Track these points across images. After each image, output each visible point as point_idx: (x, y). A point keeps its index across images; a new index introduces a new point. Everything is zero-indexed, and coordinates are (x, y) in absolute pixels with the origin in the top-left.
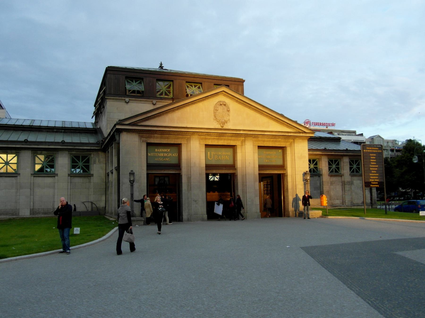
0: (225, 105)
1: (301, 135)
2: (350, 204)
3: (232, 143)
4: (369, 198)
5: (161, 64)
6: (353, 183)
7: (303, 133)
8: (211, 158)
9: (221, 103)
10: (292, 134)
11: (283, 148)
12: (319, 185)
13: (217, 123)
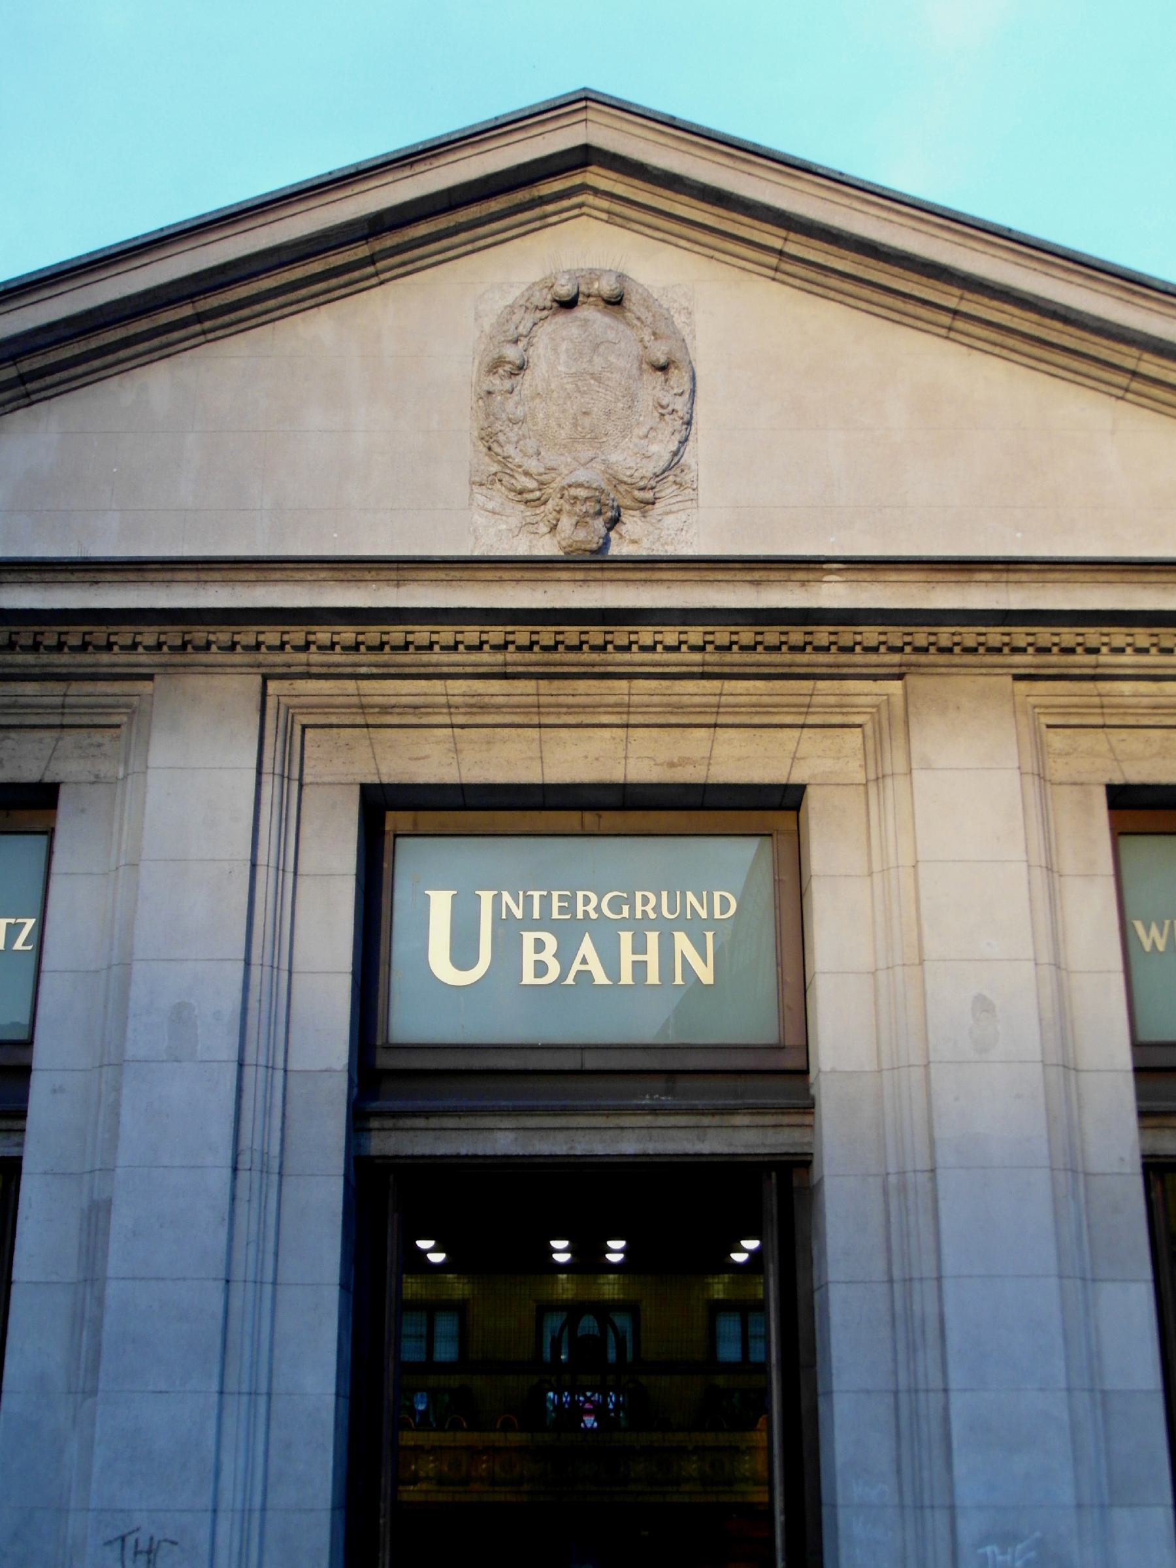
0: (615, 302)
3: (739, 759)
8: (463, 955)
9: (565, 289)
13: (517, 513)
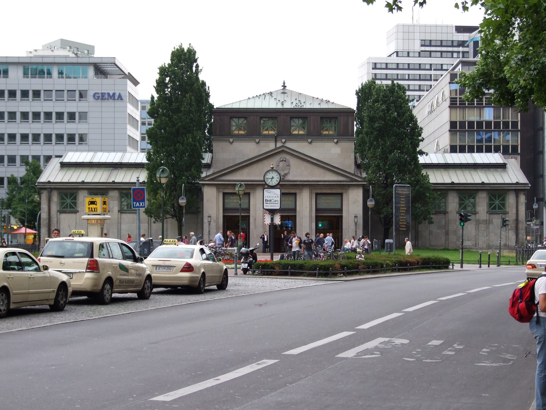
1: (354, 183)
2: (485, 246)
3: (293, 191)
4: (514, 241)
5: (284, 83)
6: (492, 222)
7: (355, 182)
10: (345, 183)
11: (341, 194)
12: (444, 223)
